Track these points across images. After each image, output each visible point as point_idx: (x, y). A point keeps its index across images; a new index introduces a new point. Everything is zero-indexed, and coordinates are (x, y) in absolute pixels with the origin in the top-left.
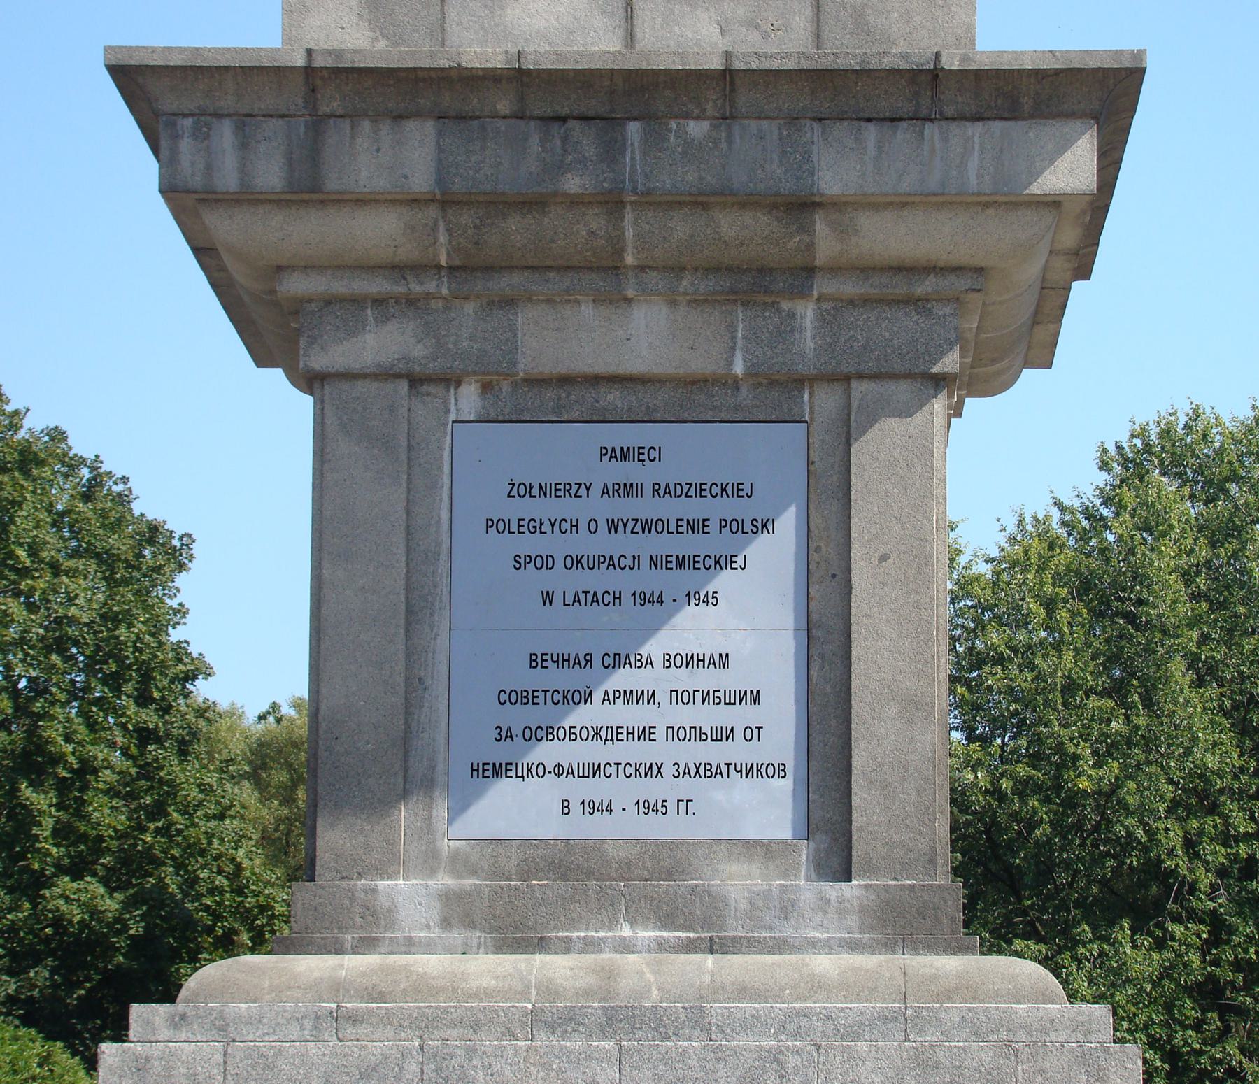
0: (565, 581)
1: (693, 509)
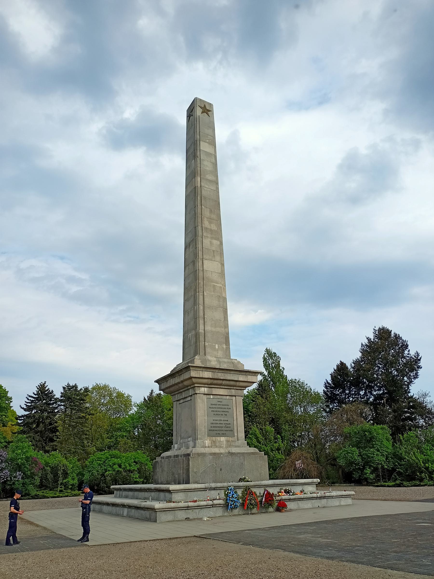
0: (216, 413)
1: (225, 407)
